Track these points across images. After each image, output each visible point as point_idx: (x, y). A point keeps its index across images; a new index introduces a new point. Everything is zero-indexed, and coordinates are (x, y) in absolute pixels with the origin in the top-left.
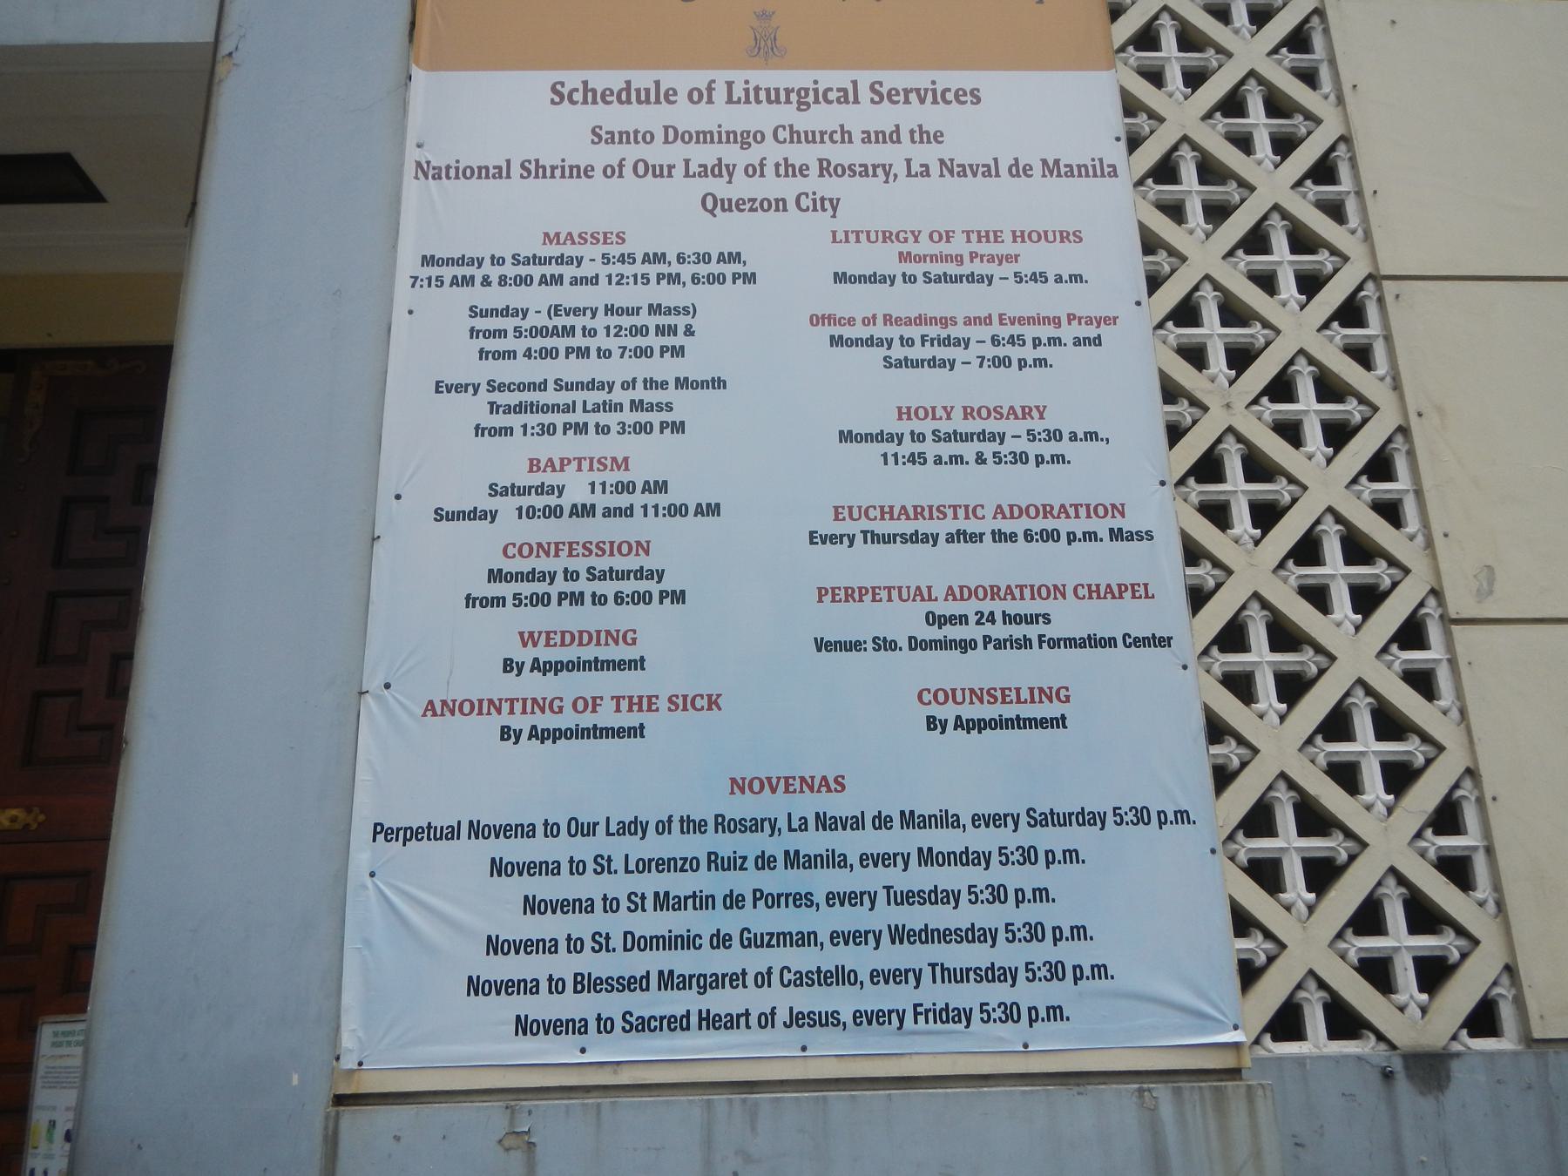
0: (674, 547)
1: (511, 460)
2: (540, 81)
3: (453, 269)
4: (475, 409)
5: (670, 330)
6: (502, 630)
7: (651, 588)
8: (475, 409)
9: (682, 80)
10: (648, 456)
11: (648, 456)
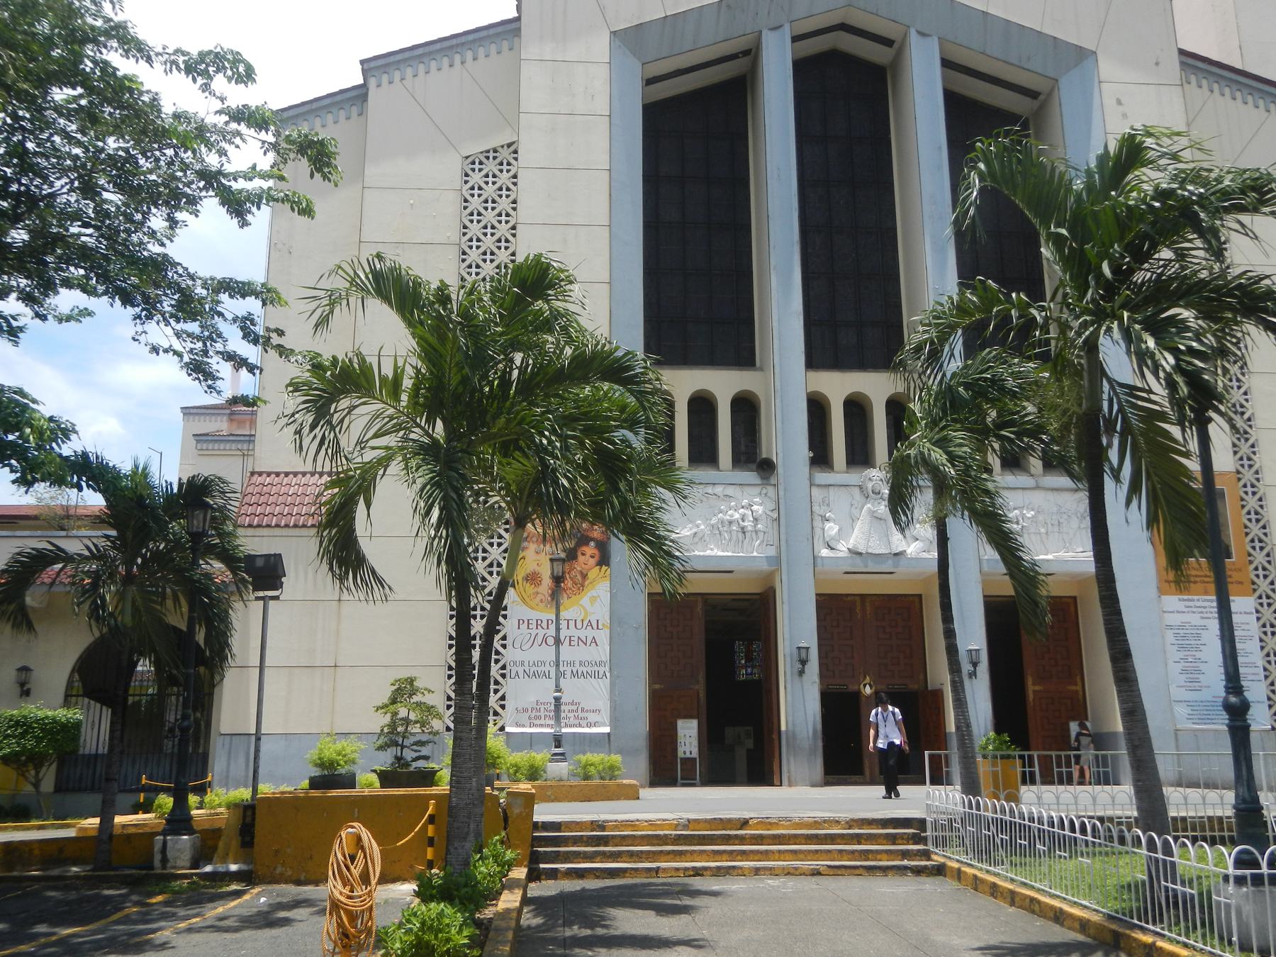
0: (1203, 667)
1: (1181, 655)
2: (1176, 597)
3: (1170, 627)
4: (1176, 647)
5: (1198, 636)
6: (1183, 677)
7: (1200, 672)
8: (1176, 647)
9: (1196, 597)
10: (1198, 655)
11: (1198, 655)
